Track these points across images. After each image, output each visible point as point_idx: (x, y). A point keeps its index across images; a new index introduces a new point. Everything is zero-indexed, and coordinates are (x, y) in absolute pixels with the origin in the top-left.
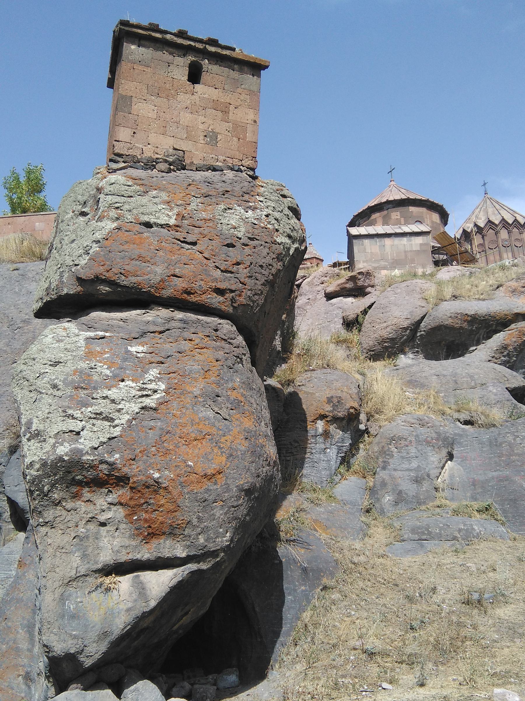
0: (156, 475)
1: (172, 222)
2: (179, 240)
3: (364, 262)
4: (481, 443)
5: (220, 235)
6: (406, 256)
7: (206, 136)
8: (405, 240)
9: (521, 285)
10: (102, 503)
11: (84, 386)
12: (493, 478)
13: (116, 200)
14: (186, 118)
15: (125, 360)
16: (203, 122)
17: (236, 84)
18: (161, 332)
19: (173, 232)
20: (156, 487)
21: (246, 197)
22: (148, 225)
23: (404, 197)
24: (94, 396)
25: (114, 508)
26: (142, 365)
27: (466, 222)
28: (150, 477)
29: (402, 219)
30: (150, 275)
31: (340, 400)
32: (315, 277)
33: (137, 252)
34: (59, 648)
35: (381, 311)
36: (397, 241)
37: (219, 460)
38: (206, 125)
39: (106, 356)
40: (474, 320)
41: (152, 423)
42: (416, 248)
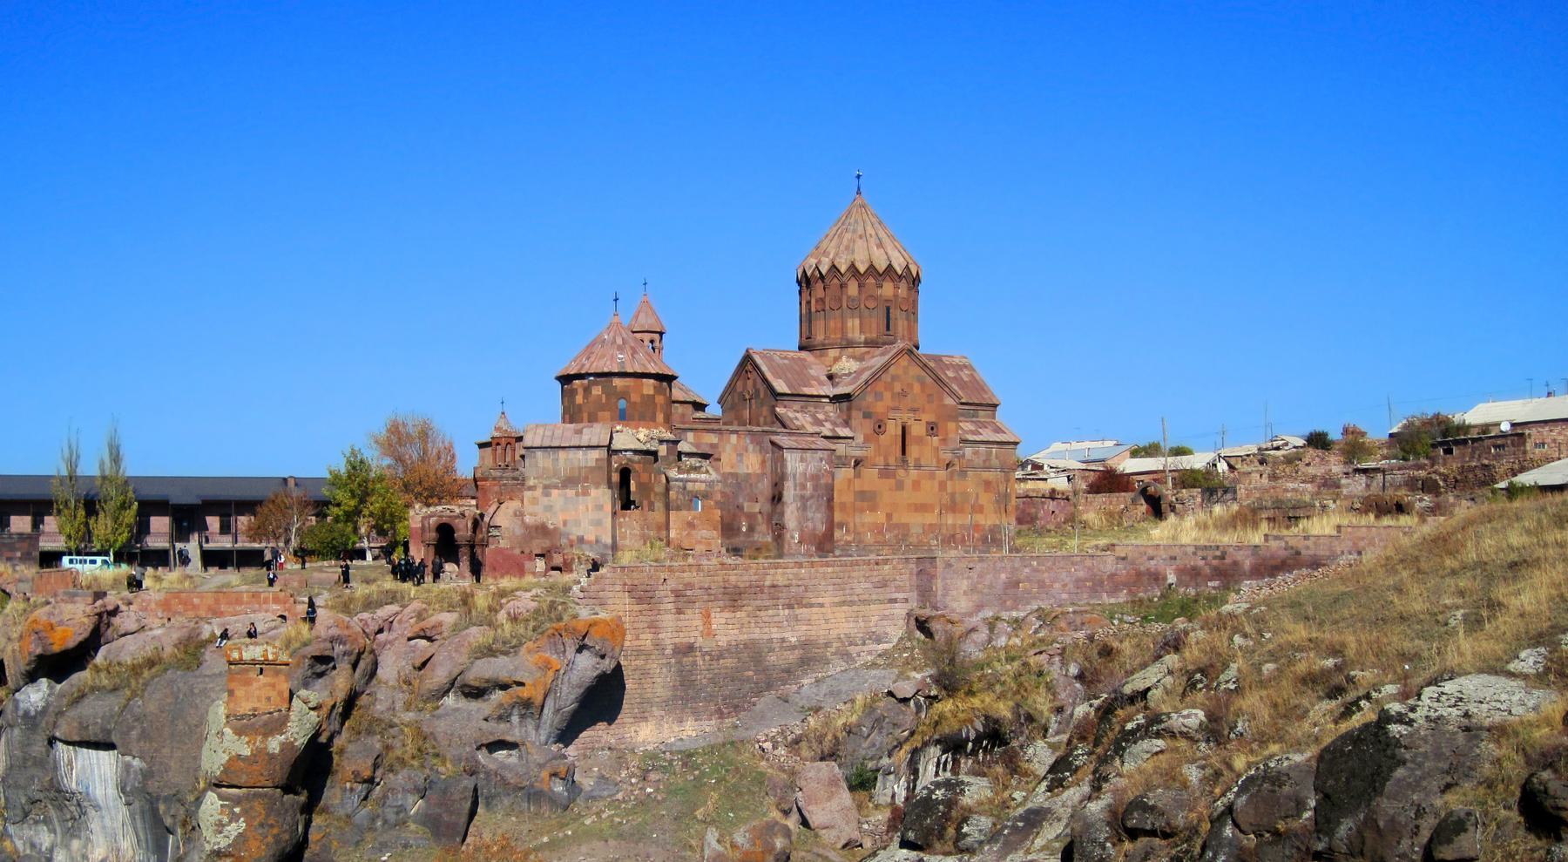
8: (580, 453)
11: (220, 826)
30: (243, 779)
36: (572, 454)
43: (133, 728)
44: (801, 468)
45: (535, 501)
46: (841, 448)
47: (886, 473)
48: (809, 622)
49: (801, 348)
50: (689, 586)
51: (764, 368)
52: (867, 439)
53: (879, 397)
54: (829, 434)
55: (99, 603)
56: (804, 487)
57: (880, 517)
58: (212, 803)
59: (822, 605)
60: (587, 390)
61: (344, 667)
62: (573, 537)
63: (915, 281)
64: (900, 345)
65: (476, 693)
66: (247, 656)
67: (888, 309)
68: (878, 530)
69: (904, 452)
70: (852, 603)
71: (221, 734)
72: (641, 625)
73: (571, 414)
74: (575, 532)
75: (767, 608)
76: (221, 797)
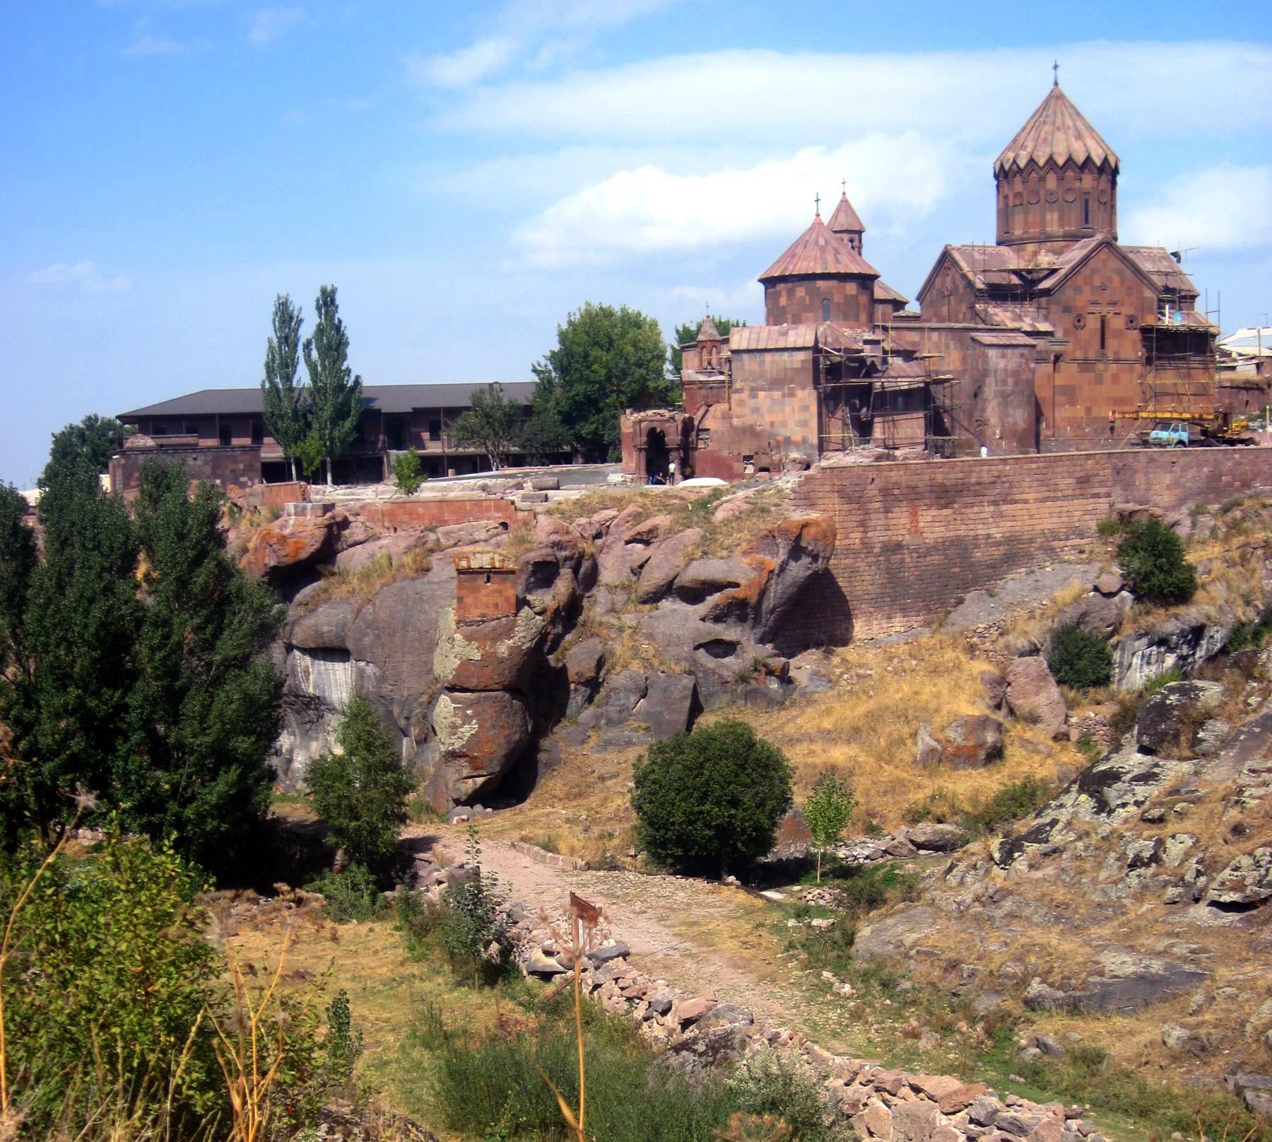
5: (497, 658)
8: (786, 354)
10: (463, 761)
11: (454, 728)
14: (485, 600)
16: (492, 600)
17: (504, 581)
20: (476, 758)
30: (473, 683)
34: (455, 797)
36: (777, 356)
40: (704, 583)
42: (798, 365)
43: (366, 635)
44: (1002, 364)
45: (741, 403)
46: (1040, 343)
47: (1086, 364)
48: (1013, 518)
49: (999, 244)
50: (897, 485)
51: (963, 264)
52: (1066, 333)
53: (1078, 290)
54: (1029, 329)
55: (329, 515)
56: (1004, 382)
57: (1080, 410)
58: (445, 706)
59: (1026, 501)
60: (791, 293)
61: (566, 572)
62: (780, 438)
63: (1115, 171)
64: (1099, 237)
65: (694, 594)
66: (475, 564)
67: (1087, 201)
68: (1075, 423)
69: (1103, 346)
70: (1056, 499)
71: (451, 640)
72: (849, 524)
73: (775, 315)
74: (782, 433)
75: (972, 505)
76: (454, 701)
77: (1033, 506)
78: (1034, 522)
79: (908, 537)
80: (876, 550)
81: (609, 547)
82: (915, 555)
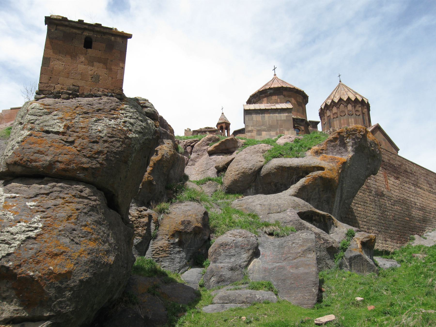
0: (32, 274)
1: (61, 130)
2: (63, 140)
3: (251, 126)
4: (275, 247)
6: (277, 123)
7: (92, 78)
9: (321, 148)
12: (275, 267)
13: (32, 118)
15: (23, 210)
18: (47, 194)
19: (61, 136)
21: (113, 112)
22: (48, 132)
23: (280, 86)
24: (2, 230)
25: (10, 290)
26: (33, 212)
27: (328, 99)
28: (28, 275)
29: (279, 99)
31: (189, 222)
32: (203, 141)
33: (38, 149)
35: (236, 164)
37: (69, 267)
38: (93, 71)
39: (14, 208)
41: (31, 246)
77: (427, 193)
78: (429, 202)
79: (385, 190)
80: (373, 192)
81: (194, 161)
82: (390, 203)
